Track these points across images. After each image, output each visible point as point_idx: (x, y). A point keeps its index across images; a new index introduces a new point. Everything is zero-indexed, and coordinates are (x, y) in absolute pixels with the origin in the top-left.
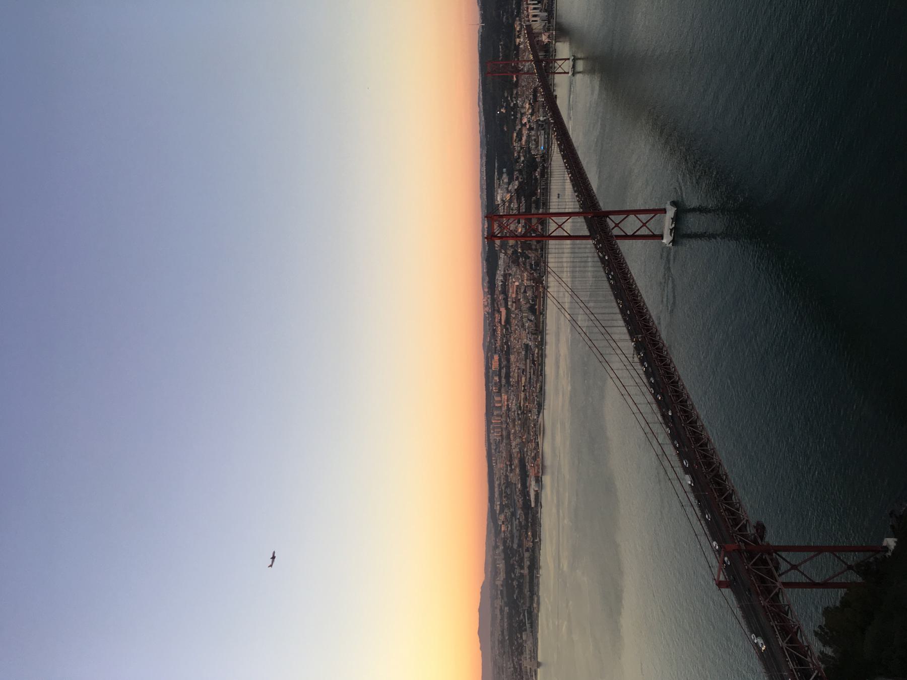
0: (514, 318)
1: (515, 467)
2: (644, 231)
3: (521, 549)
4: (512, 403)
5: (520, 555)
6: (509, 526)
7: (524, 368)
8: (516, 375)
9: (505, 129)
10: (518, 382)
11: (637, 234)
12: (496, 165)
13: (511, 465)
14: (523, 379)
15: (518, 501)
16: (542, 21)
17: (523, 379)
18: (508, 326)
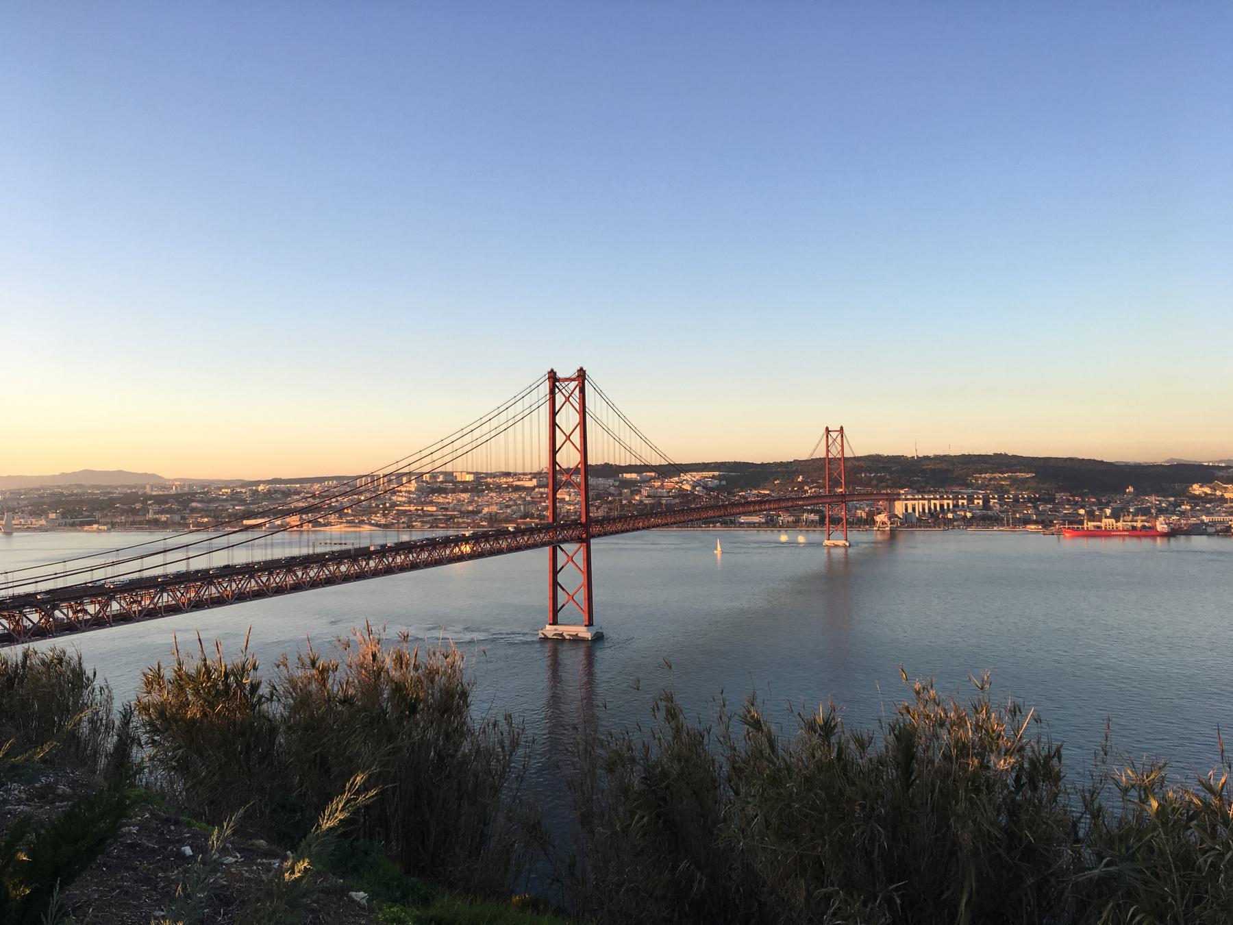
0: (520, 495)
1: (309, 502)
2: (562, 598)
3: (188, 511)
4: (402, 496)
5: (178, 510)
6: (225, 497)
7: (450, 509)
8: (441, 500)
9: (776, 482)
10: (431, 503)
11: (558, 587)
12: (732, 474)
13: (314, 496)
14: (434, 509)
15: (259, 507)
16: (906, 518)
17: (434, 509)
18: (510, 490)
